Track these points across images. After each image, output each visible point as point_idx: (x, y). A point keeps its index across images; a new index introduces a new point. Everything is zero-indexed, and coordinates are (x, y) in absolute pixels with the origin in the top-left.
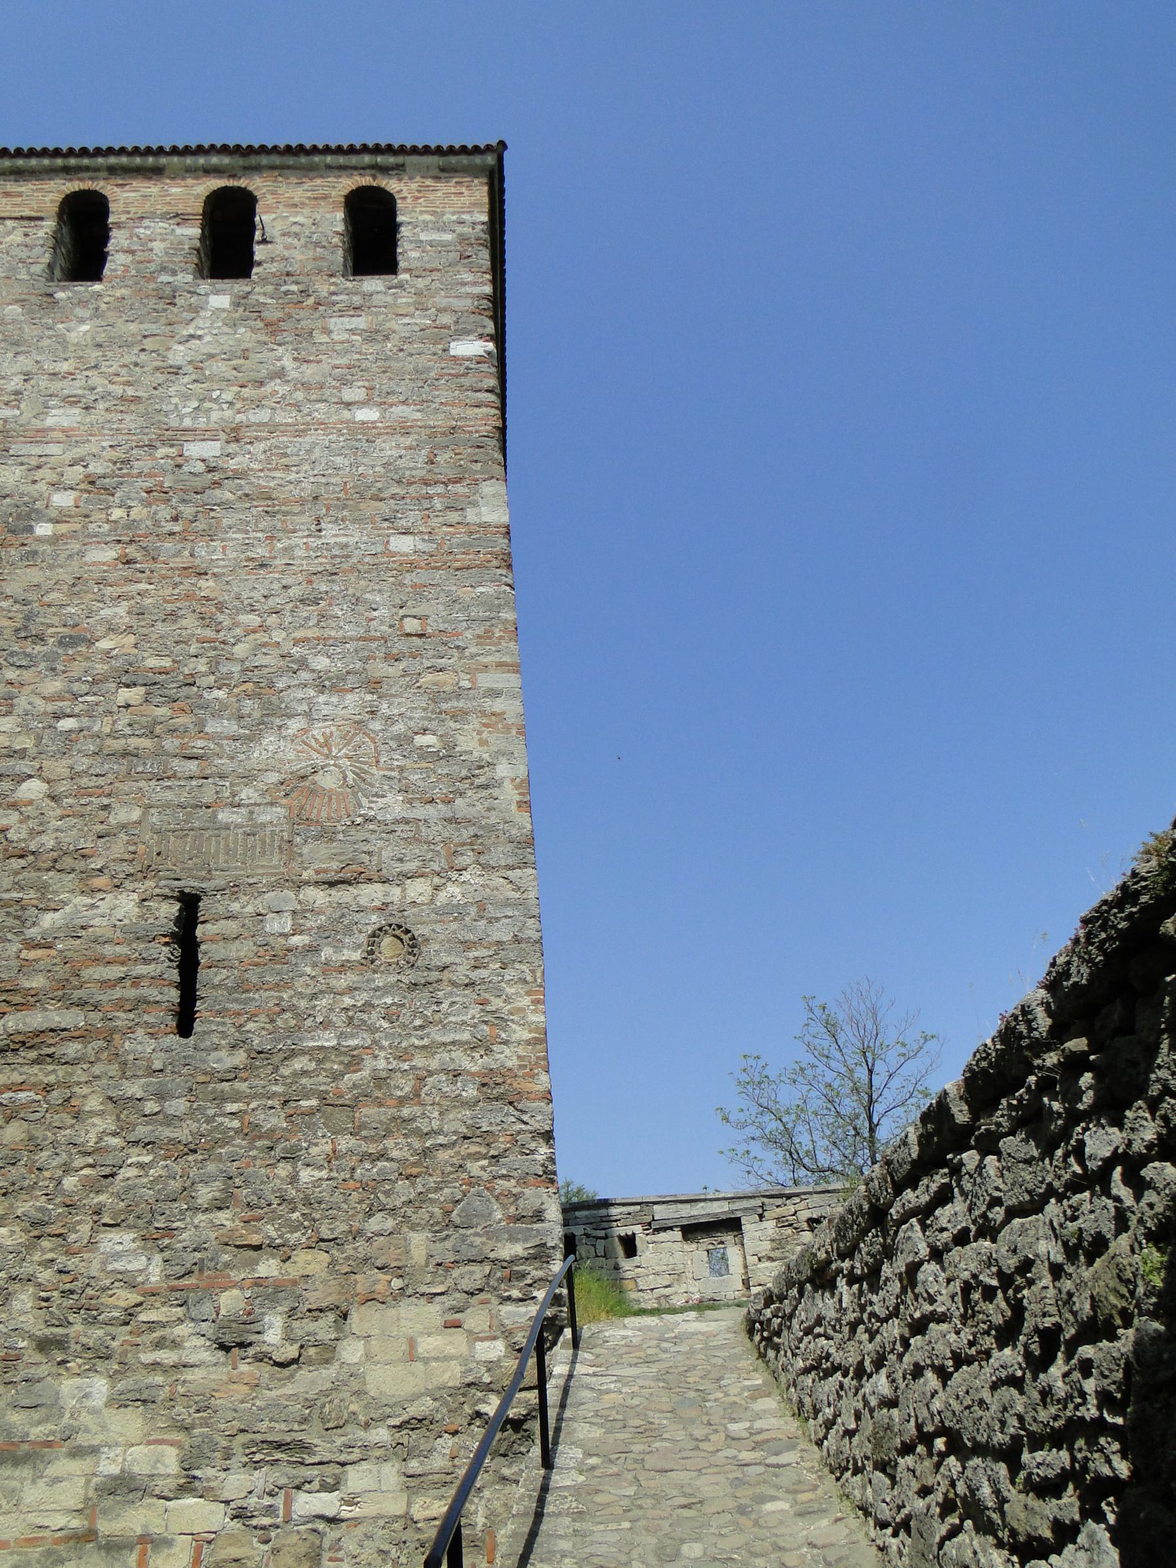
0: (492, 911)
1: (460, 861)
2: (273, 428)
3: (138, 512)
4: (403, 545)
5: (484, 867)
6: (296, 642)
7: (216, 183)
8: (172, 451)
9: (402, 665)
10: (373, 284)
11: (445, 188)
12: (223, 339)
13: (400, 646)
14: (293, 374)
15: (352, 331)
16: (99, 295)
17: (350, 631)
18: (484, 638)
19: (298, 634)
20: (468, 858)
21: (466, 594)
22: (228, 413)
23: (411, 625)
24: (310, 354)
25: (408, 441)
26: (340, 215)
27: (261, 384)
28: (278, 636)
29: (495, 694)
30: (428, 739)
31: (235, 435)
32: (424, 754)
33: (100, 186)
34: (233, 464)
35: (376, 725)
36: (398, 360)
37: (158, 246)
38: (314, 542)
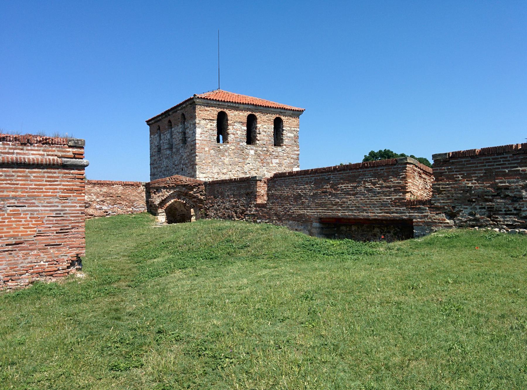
7: (249, 113)
10: (279, 149)
12: (254, 164)
15: (277, 163)
16: (229, 148)
24: (269, 170)
26: (273, 126)
33: (225, 110)
37: (238, 132)
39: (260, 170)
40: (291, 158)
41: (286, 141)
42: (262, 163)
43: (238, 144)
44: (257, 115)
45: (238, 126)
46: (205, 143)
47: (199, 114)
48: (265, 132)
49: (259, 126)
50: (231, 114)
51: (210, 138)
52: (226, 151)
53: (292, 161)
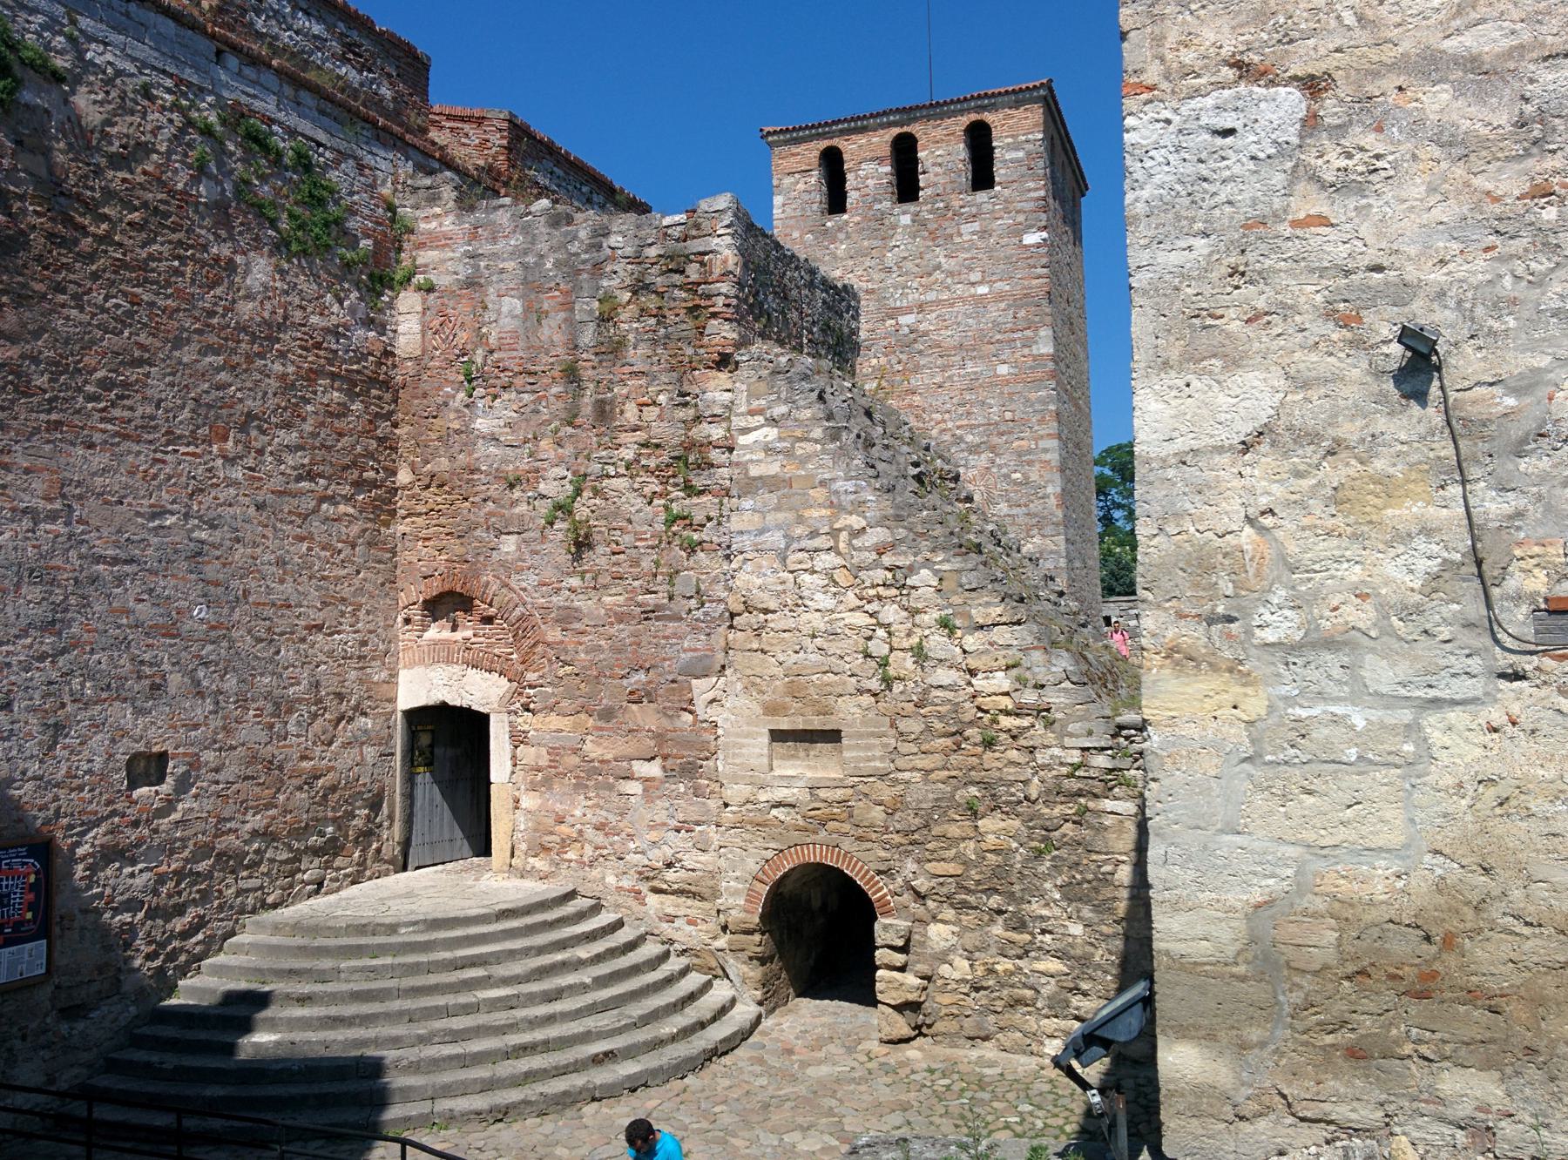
0: (1045, 556)
1: (1032, 533)
2: (938, 302)
3: (883, 360)
4: (1003, 370)
5: (1043, 536)
6: (958, 428)
7: (896, 131)
8: (893, 322)
9: (1004, 438)
10: (982, 196)
11: (1019, 113)
12: (909, 247)
13: (1003, 428)
14: (945, 266)
15: (973, 233)
16: (847, 222)
17: (981, 420)
18: (1041, 421)
19: (958, 423)
20: (1035, 531)
21: (1033, 396)
22: (916, 295)
23: (1008, 415)
25: (1003, 305)
27: (930, 275)
28: (950, 425)
29: (1046, 451)
30: (1018, 475)
31: (921, 308)
32: (1015, 483)
33: (835, 142)
34: (922, 327)
35: (994, 470)
36: (997, 251)
37: (869, 182)
38: (962, 372)
39: (927, 256)
40: (1018, 212)
41: (1000, 172)
42: (933, 240)
43: (870, 208)
44: (915, 129)
45: (868, 168)
46: (792, 222)
47: (778, 165)
48: (940, 165)
49: (921, 155)
50: (851, 147)
51: (803, 209)
52: (840, 229)
53: (1021, 218)
